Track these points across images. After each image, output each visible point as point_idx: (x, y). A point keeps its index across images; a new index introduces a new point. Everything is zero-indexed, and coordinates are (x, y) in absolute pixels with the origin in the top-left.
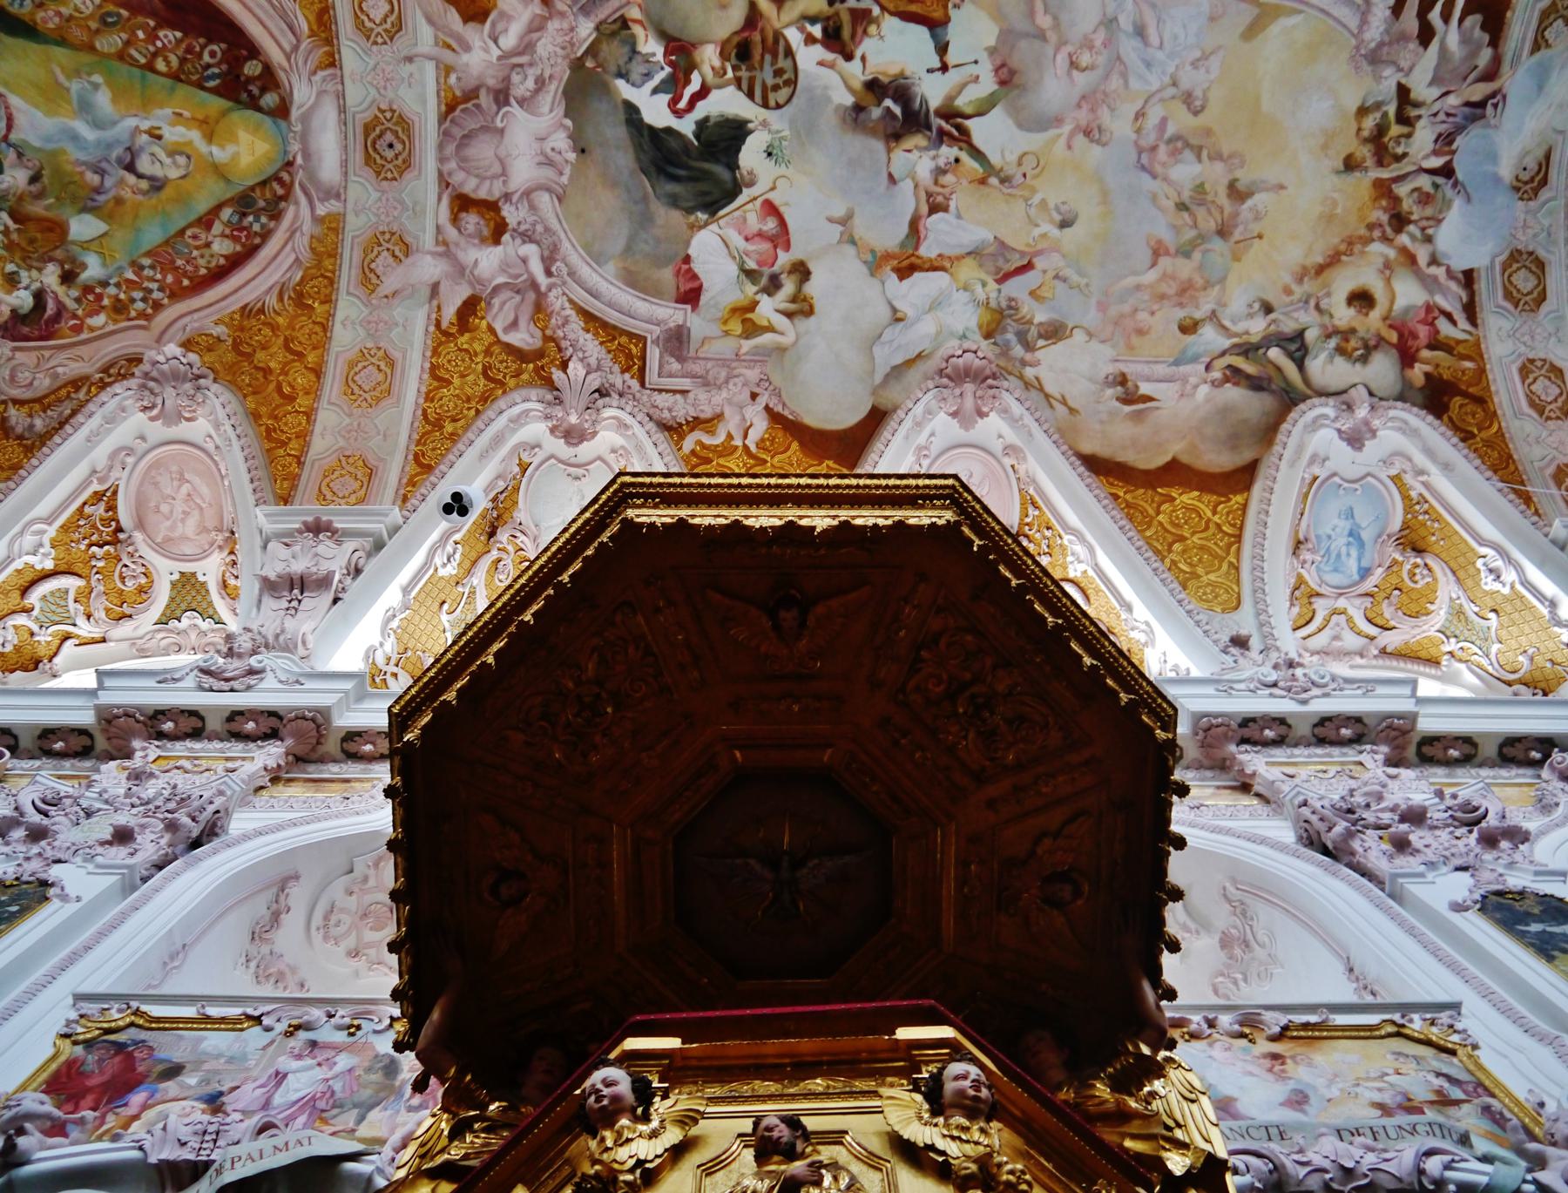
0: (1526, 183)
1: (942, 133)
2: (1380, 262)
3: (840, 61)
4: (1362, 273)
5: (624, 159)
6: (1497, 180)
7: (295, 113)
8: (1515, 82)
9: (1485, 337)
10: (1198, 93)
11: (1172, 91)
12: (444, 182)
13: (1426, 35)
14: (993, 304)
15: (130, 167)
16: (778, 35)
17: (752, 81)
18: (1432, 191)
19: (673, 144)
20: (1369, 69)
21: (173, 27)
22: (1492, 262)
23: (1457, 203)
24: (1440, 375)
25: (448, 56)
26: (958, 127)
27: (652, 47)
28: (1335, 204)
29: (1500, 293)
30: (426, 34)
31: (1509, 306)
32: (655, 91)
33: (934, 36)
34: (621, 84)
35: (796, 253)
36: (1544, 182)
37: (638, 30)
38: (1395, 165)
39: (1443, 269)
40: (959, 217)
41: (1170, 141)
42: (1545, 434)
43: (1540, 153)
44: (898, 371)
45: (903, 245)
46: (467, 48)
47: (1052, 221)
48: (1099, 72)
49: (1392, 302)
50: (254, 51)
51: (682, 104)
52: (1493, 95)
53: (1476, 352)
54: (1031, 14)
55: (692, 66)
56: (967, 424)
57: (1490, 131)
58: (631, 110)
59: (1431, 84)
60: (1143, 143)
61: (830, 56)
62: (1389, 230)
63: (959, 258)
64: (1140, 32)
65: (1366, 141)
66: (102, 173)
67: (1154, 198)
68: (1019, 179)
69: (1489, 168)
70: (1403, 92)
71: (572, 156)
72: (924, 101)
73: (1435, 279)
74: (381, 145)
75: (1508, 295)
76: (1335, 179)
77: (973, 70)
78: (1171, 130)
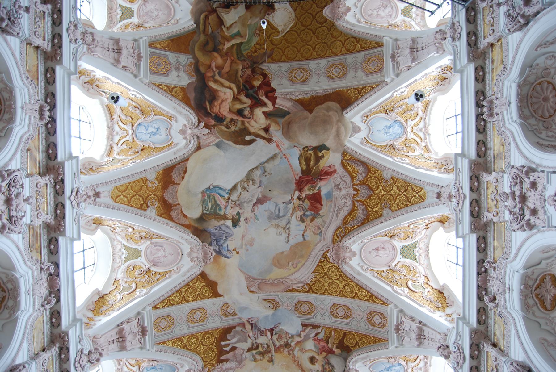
0: (274, 306)
2: (300, 352)
4: (304, 359)
6: (273, 315)
8: (244, 317)
9: (323, 324)
13: (234, 349)
18: (278, 335)
20: (243, 362)
22: (299, 317)
23: (281, 327)
24: (337, 343)
28: (283, 365)
29: (309, 316)
31: (313, 314)
36: (273, 300)
38: (270, 347)
39: (302, 333)
42: (356, 318)
43: (265, 302)
49: (313, 351)
52: (249, 322)
53: (329, 330)
57: (259, 321)
59: (247, 342)
62: (290, 349)
65: (264, 357)
69: (270, 317)
70: (249, 350)
73: (305, 336)
75: (309, 314)
76: (274, 365)
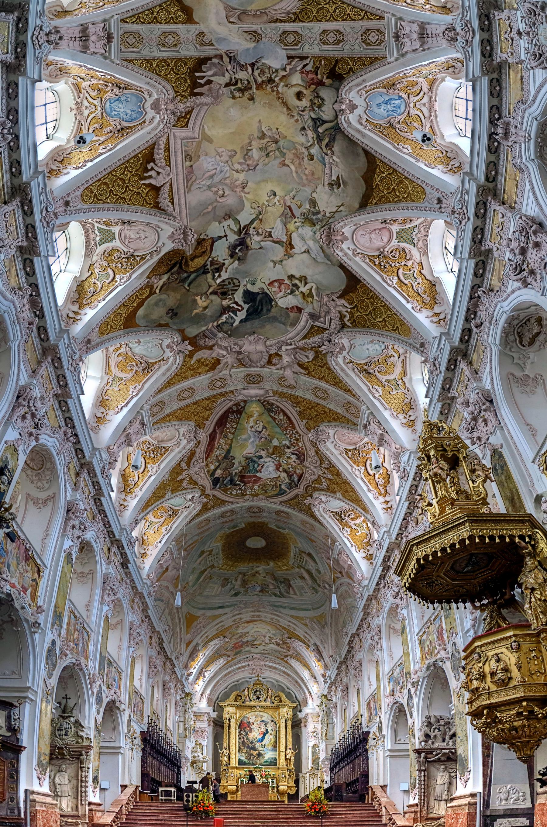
1: (245, 234)
3: (225, 266)
5: (256, 322)
7: (246, 399)
10: (229, 154)
11: (230, 162)
12: (263, 367)
14: (303, 221)
15: (260, 432)
16: (219, 285)
17: (232, 290)
19: (251, 310)
21: (226, 425)
25: (229, 367)
26: (244, 229)
27: (224, 318)
30: (223, 372)
32: (236, 316)
33: (217, 241)
34: (234, 325)
35: (285, 278)
37: (220, 322)
40: (273, 228)
41: (246, 161)
44: (327, 256)
45: (283, 246)
46: (227, 362)
47: (274, 198)
48: (225, 187)
50: (231, 408)
51: (240, 308)
54: (208, 212)
55: (229, 307)
56: (346, 239)
58: (241, 321)
60: (246, 169)
61: (224, 269)
63: (287, 229)
64: (212, 177)
66: (262, 438)
67: (266, 165)
68: (260, 209)
71: (256, 335)
72: (236, 240)
74: (253, 380)
77: (226, 228)
78: (242, 161)
